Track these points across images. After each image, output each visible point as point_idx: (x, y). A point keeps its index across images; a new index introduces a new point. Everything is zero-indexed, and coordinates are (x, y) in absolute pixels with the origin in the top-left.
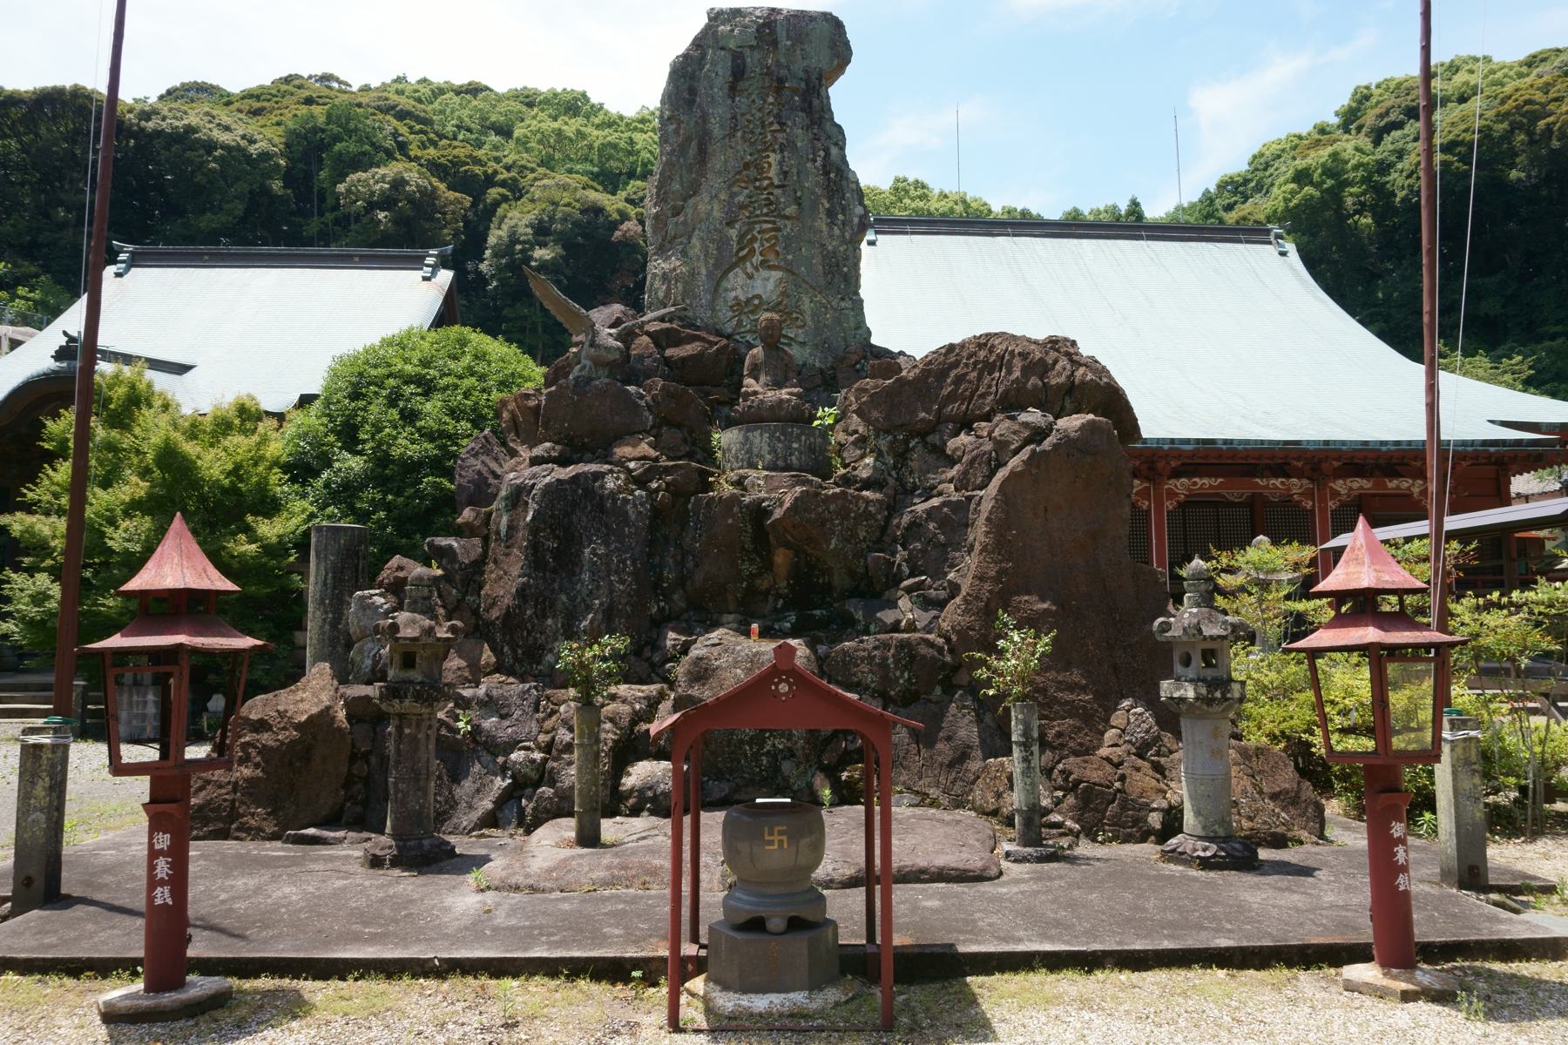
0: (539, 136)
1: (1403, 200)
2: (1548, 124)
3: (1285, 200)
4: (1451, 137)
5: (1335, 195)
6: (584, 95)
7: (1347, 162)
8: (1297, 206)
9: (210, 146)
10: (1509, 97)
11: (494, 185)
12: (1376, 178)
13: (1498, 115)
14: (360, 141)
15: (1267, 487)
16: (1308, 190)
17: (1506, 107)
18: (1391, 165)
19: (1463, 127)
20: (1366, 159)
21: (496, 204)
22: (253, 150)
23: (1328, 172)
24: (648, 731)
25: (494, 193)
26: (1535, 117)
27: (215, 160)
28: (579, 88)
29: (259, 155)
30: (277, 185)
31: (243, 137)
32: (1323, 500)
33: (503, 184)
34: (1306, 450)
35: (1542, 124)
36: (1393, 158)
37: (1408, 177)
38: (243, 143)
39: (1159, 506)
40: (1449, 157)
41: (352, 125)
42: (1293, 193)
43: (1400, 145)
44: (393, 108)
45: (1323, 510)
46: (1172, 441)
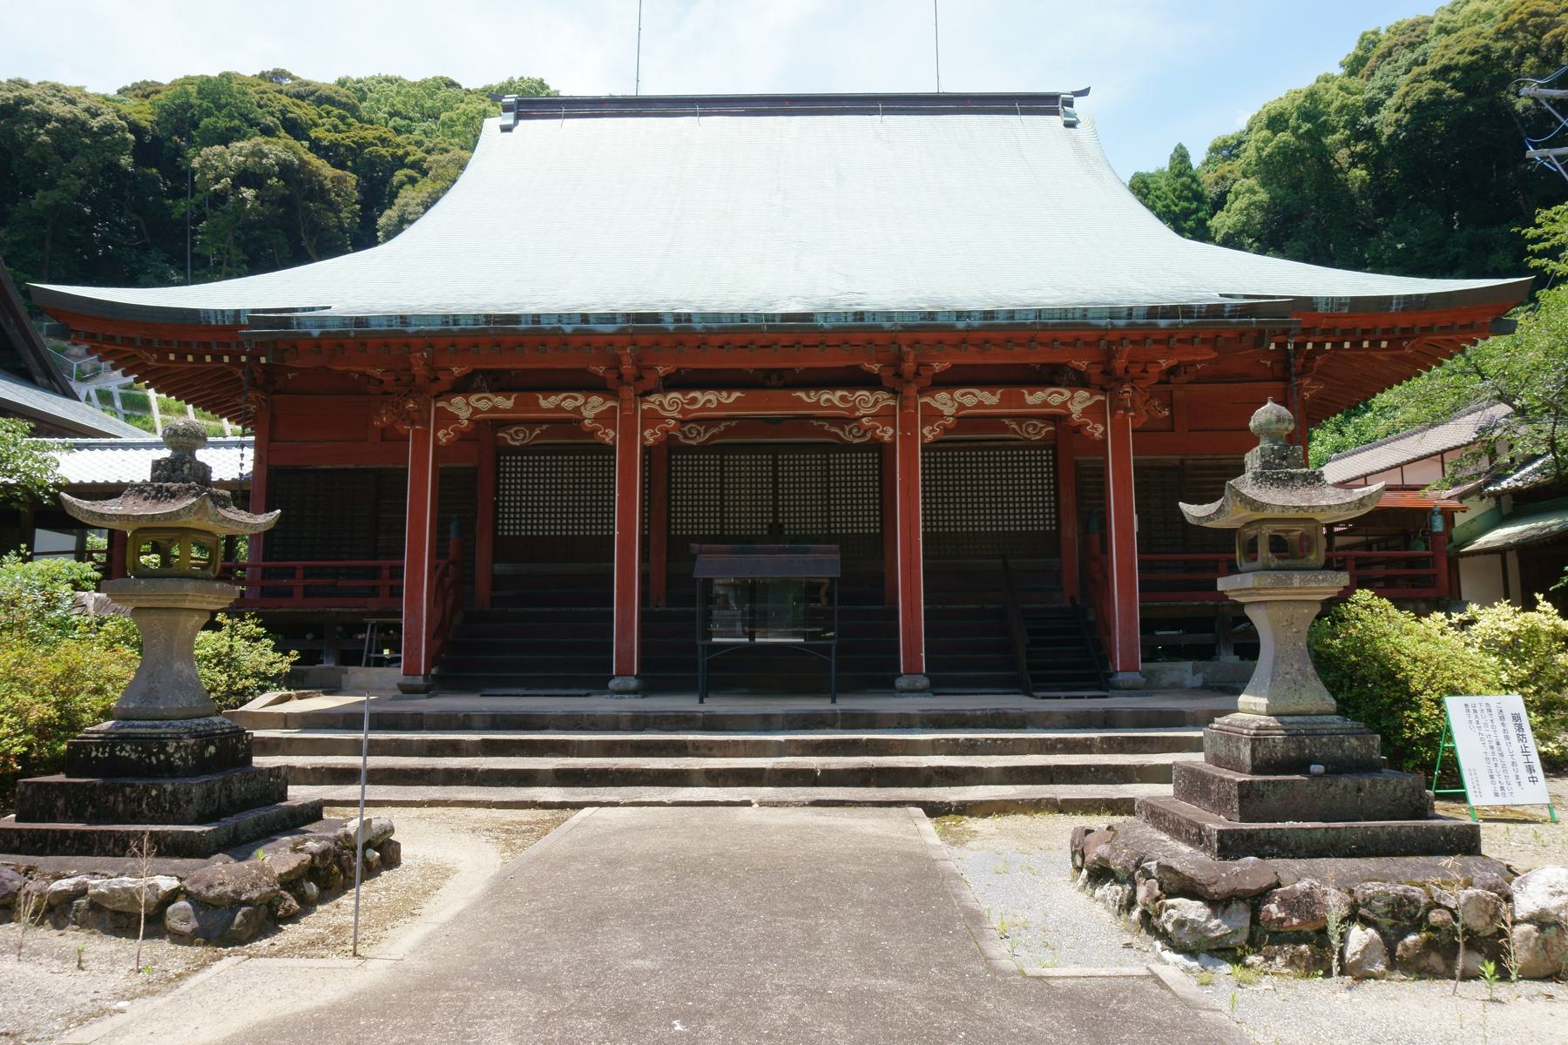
0: (463, 118)
1: (1390, 137)
2: (1555, 36)
3: (1258, 149)
4: (1444, 61)
5: (1315, 136)
6: (541, 83)
7: (1329, 104)
8: (1270, 156)
9: (43, 119)
10: (1513, 12)
11: (403, 166)
12: (1365, 120)
13: (1498, 32)
14: (231, 117)
15: (816, 405)
16: (1284, 136)
17: (1509, 22)
18: (1381, 103)
19: (1458, 48)
20: (1351, 100)
21: (401, 185)
22: (95, 124)
23: (1306, 115)
24: (18, 820)
25: (400, 175)
26: (1543, 29)
27: (48, 132)
28: (537, 77)
29: (101, 128)
30: (126, 161)
31: (87, 110)
32: (908, 424)
33: (413, 165)
34: (879, 329)
35: (1547, 37)
36: (1382, 96)
37: (1397, 110)
38: (84, 116)
39: (628, 437)
40: (1441, 85)
41: (223, 101)
42: (1266, 141)
43: (1389, 81)
44: (313, 93)
45: (909, 442)
46: (585, 318)
